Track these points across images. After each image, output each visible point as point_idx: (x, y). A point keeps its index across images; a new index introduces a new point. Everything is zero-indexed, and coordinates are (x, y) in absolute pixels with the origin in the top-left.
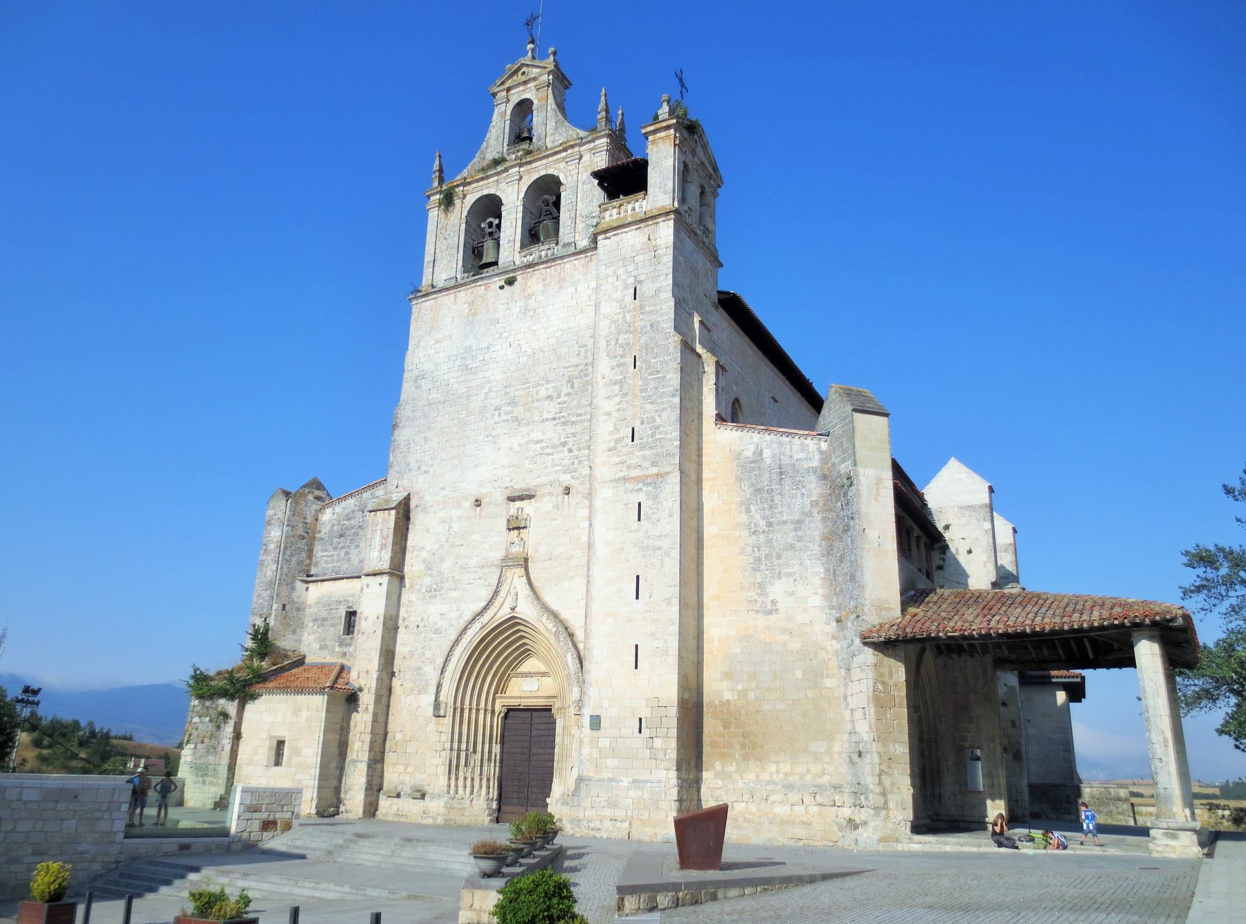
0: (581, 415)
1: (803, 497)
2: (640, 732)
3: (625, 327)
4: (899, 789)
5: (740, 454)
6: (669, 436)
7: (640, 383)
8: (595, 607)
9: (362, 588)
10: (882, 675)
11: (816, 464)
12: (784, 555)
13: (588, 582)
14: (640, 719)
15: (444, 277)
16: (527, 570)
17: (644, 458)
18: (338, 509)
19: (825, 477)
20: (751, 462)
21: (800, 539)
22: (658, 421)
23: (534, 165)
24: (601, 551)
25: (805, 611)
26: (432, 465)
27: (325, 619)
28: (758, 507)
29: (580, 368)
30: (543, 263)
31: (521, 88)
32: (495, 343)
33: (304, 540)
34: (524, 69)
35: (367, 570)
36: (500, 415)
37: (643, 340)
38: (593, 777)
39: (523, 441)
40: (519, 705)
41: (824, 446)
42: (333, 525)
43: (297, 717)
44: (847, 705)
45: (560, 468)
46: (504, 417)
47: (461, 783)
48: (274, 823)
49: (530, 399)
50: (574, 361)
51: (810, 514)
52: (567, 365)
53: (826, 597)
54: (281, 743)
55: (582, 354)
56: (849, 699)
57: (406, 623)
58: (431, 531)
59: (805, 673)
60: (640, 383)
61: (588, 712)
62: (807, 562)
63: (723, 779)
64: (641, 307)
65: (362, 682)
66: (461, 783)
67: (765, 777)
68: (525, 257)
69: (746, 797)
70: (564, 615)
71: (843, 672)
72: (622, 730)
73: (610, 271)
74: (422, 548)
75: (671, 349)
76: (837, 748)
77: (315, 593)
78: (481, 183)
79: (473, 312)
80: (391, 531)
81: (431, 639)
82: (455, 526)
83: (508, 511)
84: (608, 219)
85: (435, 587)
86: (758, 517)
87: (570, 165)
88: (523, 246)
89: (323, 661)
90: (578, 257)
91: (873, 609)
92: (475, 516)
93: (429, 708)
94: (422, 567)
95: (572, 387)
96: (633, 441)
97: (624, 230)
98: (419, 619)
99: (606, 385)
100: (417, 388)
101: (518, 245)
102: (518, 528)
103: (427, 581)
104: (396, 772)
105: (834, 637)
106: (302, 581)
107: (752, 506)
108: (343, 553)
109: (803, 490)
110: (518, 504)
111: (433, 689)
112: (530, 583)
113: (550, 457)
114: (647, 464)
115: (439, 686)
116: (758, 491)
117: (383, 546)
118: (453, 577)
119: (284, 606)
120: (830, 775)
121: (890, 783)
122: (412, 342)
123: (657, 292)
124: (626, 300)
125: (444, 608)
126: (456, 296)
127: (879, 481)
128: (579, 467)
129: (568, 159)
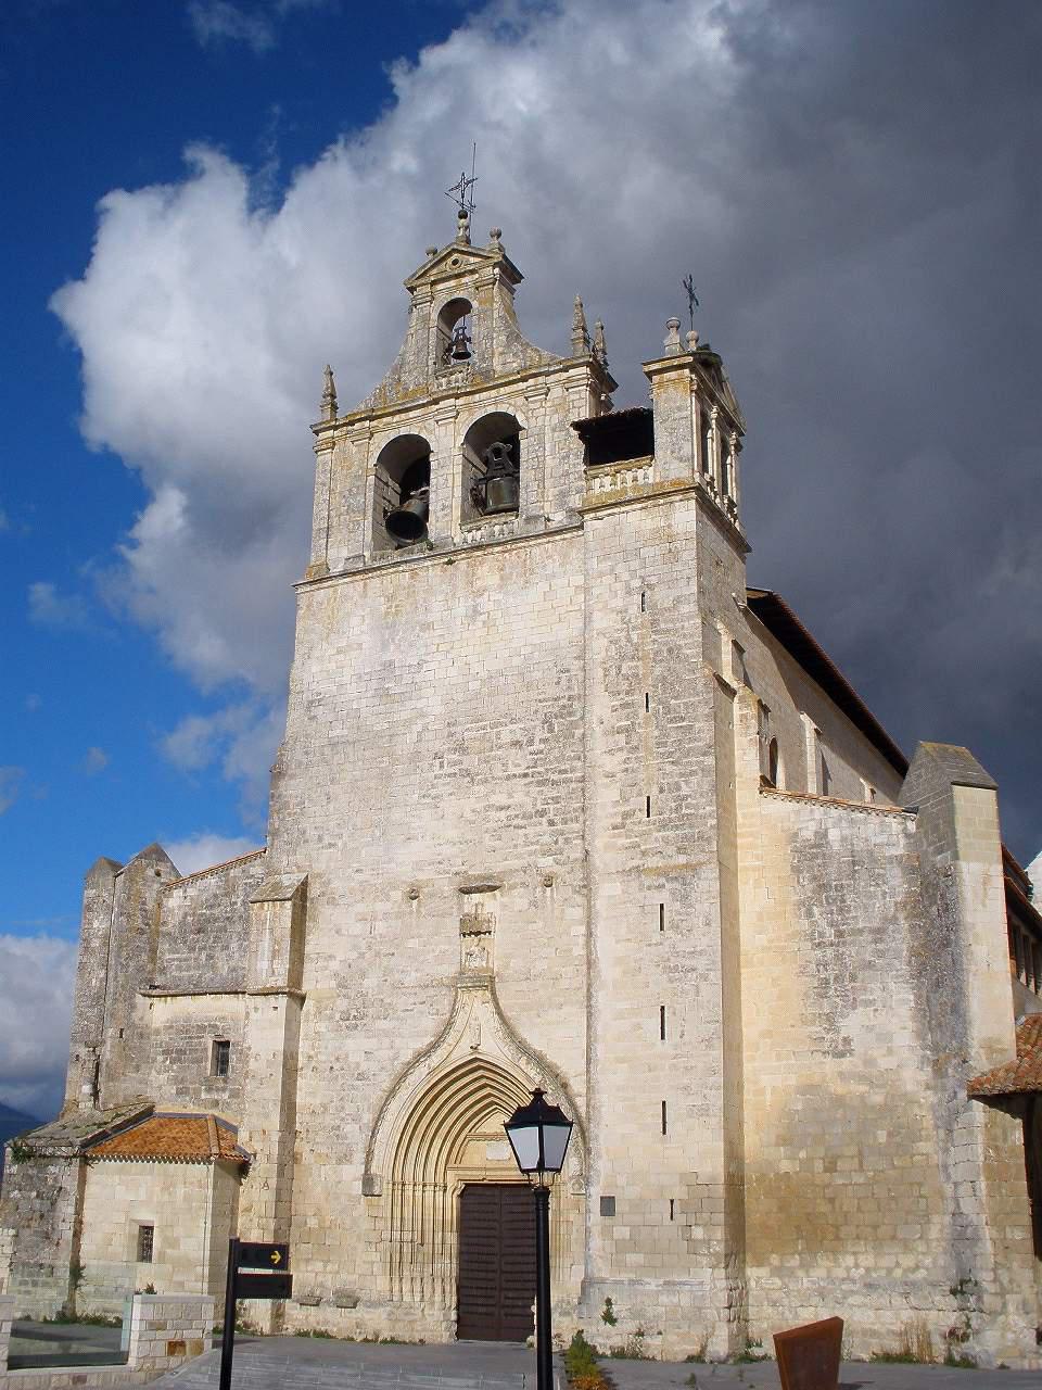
0: (565, 771)
1: (885, 898)
3: (630, 650)
5: (796, 834)
6: (701, 811)
7: (656, 733)
8: (600, 1050)
9: (248, 1013)
10: (995, 1139)
11: (900, 851)
12: (860, 977)
13: (590, 1015)
14: (672, 1201)
15: (345, 553)
16: (493, 994)
17: (666, 841)
18: (192, 892)
19: (913, 870)
20: (812, 847)
21: (881, 954)
22: (685, 790)
23: (477, 397)
24: (607, 971)
25: (890, 1051)
26: (340, 836)
27: (181, 1052)
28: (823, 909)
29: (561, 703)
30: (498, 544)
31: (452, 283)
32: (428, 658)
33: (145, 936)
34: (455, 256)
35: (252, 988)
36: (442, 766)
37: (658, 671)
38: (607, 1279)
39: (479, 806)
40: (483, 1179)
41: (912, 826)
42: (186, 915)
43: (170, 1194)
44: (948, 1177)
45: (538, 847)
46: (447, 770)
47: (406, 1287)
48: (182, 1344)
49: (488, 745)
50: (552, 691)
51: (895, 918)
52: (540, 697)
53: (920, 1035)
54: (147, 1230)
55: (564, 682)
56: (951, 1170)
57: (314, 1064)
58: (344, 932)
59: (890, 1135)
60: (656, 733)
61: (596, 1192)
62: (892, 986)
63: (781, 1278)
64: (654, 623)
65: (257, 1146)
66: (406, 1287)
67: (840, 1273)
68: (469, 532)
69: (815, 1300)
70: (552, 1057)
71: (942, 1133)
72: (647, 1216)
73: (606, 566)
74: (331, 957)
75: (700, 687)
76: (934, 1233)
77: (160, 1013)
78: (397, 418)
79: (393, 610)
80: (288, 932)
81: (353, 1087)
82: (380, 927)
83: (460, 906)
84: (597, 491)
85: (354, 1013)
86: (823, 923)
87: (532, 402)
88: (465, 518)
89: (184, 1111)
90: (551, 539)
91: (982, 1051)
92: (411, 913)
93: (357, 1183)
94: (333, 984)
95: (551, 730)
96: (648, 816)
97: (623, 509)
98: (333, 1059)
99: (605, 733)
100: (312, 718)
101: (457, 513)
102: (478, 933)
103: (342, 1004)
104: (312, 1271)
105: (928, 1087)
106: (144, 995)
107: (815, 908)
108: (203, 957)
109: (885, 888)
110: (476, 897)
111: (360, 1156)
112: (500, 1013)
113: (521, 832)
114: (671, 850)
115: (369, 1153)
116: (823, 887)
117: (275, 954)
119: (122, 1030)
120: (927, 1269)
122: (300, 651)
123: (678, 601)
124: (630, 611)
125: (371, 1044)
126: (365, 585)
127: (986, 880)
128: (566, 847)
129: (530, 394)
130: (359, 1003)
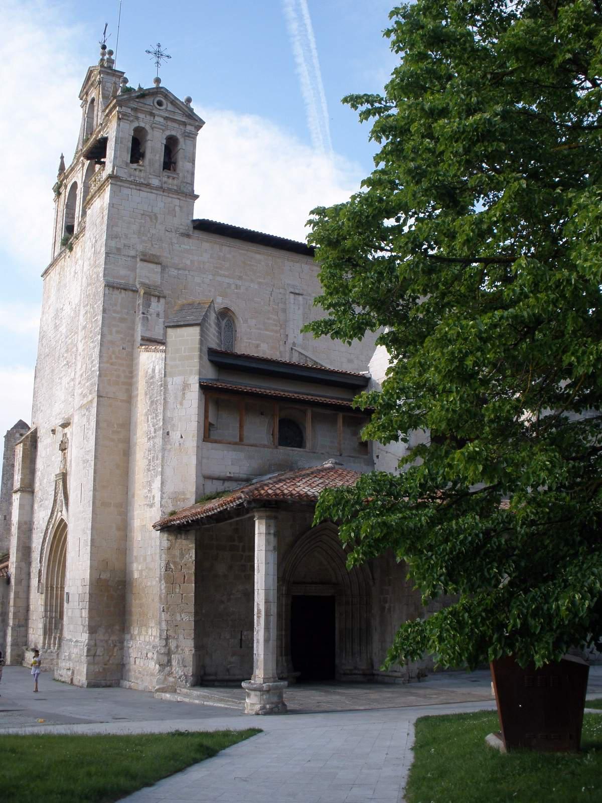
4: (182, 650)
10: (174, 556)
86: (151, 425)
116: (152, 402)
121: (175, 645)
127: (186, 386)
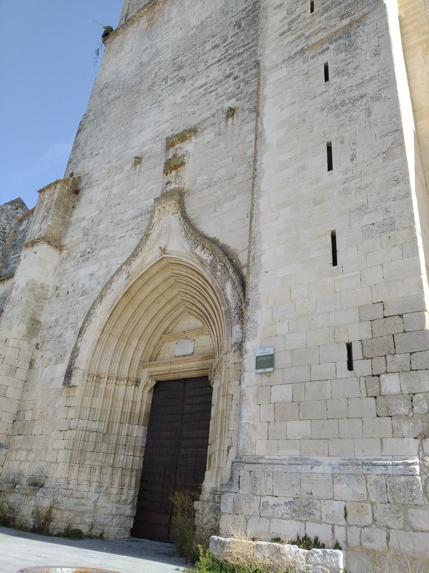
2: (350, 367)
14: (349, 347)
38: (262, 457)
45: (224, 97)
47: (84, 476)
74: (84, 219)
85: (89, 250)
98: (70, 285)
104: (17, 460)
118: (107, 236)
130: (93, 243)
